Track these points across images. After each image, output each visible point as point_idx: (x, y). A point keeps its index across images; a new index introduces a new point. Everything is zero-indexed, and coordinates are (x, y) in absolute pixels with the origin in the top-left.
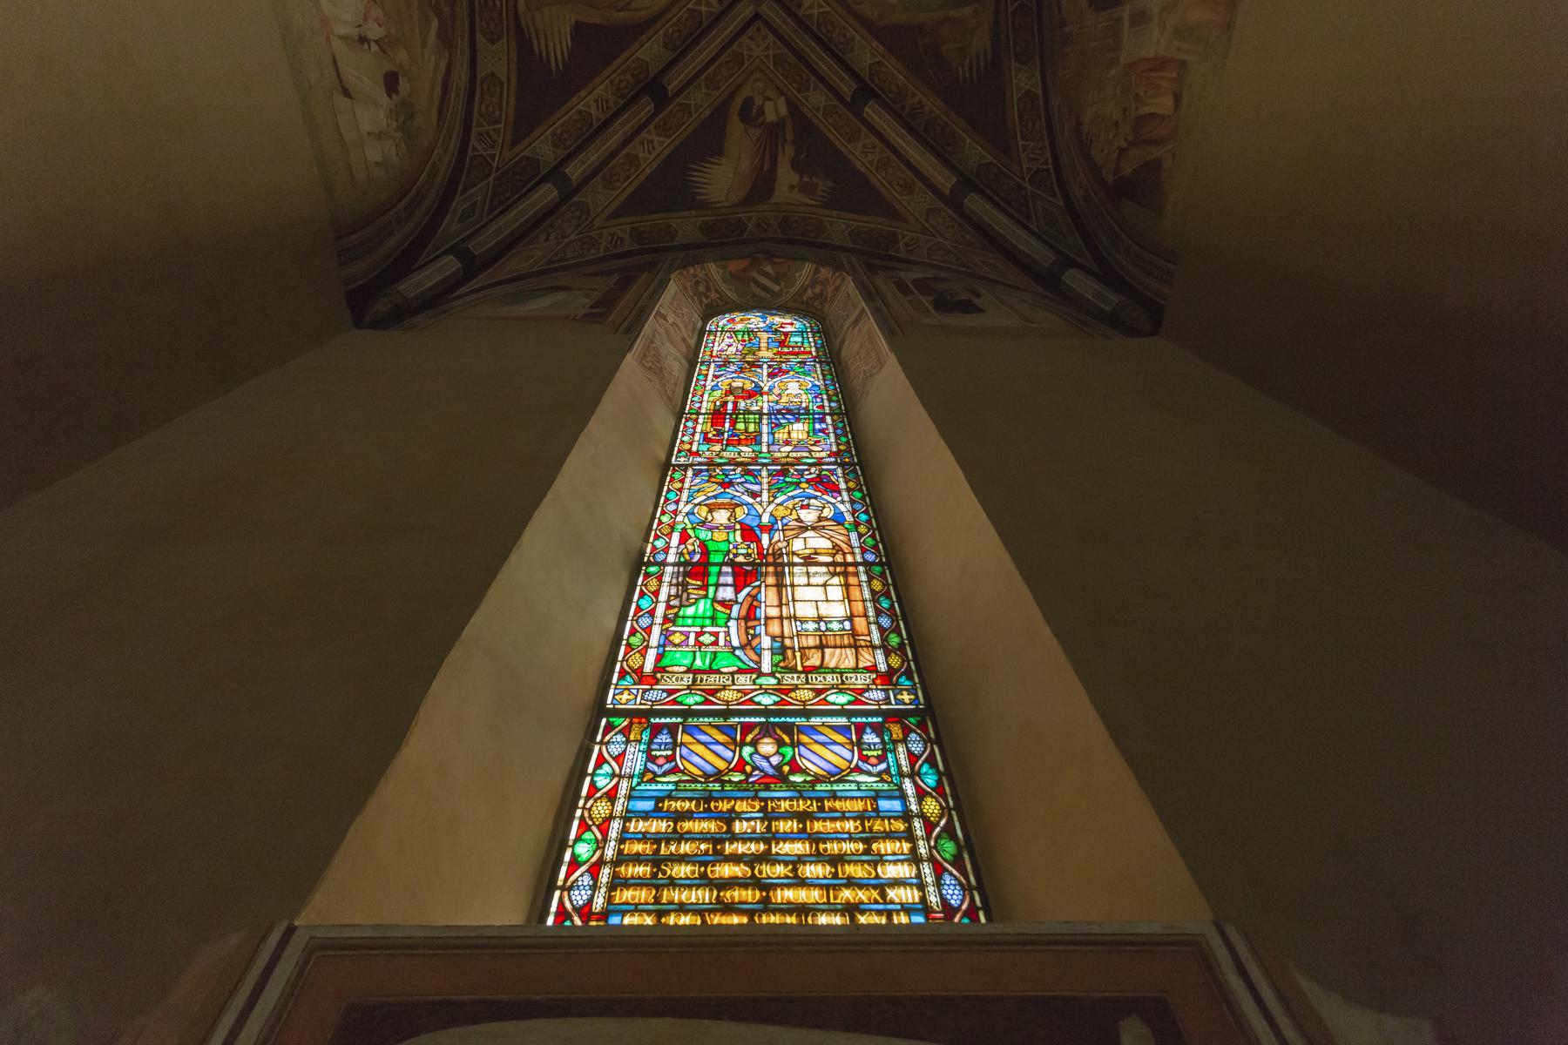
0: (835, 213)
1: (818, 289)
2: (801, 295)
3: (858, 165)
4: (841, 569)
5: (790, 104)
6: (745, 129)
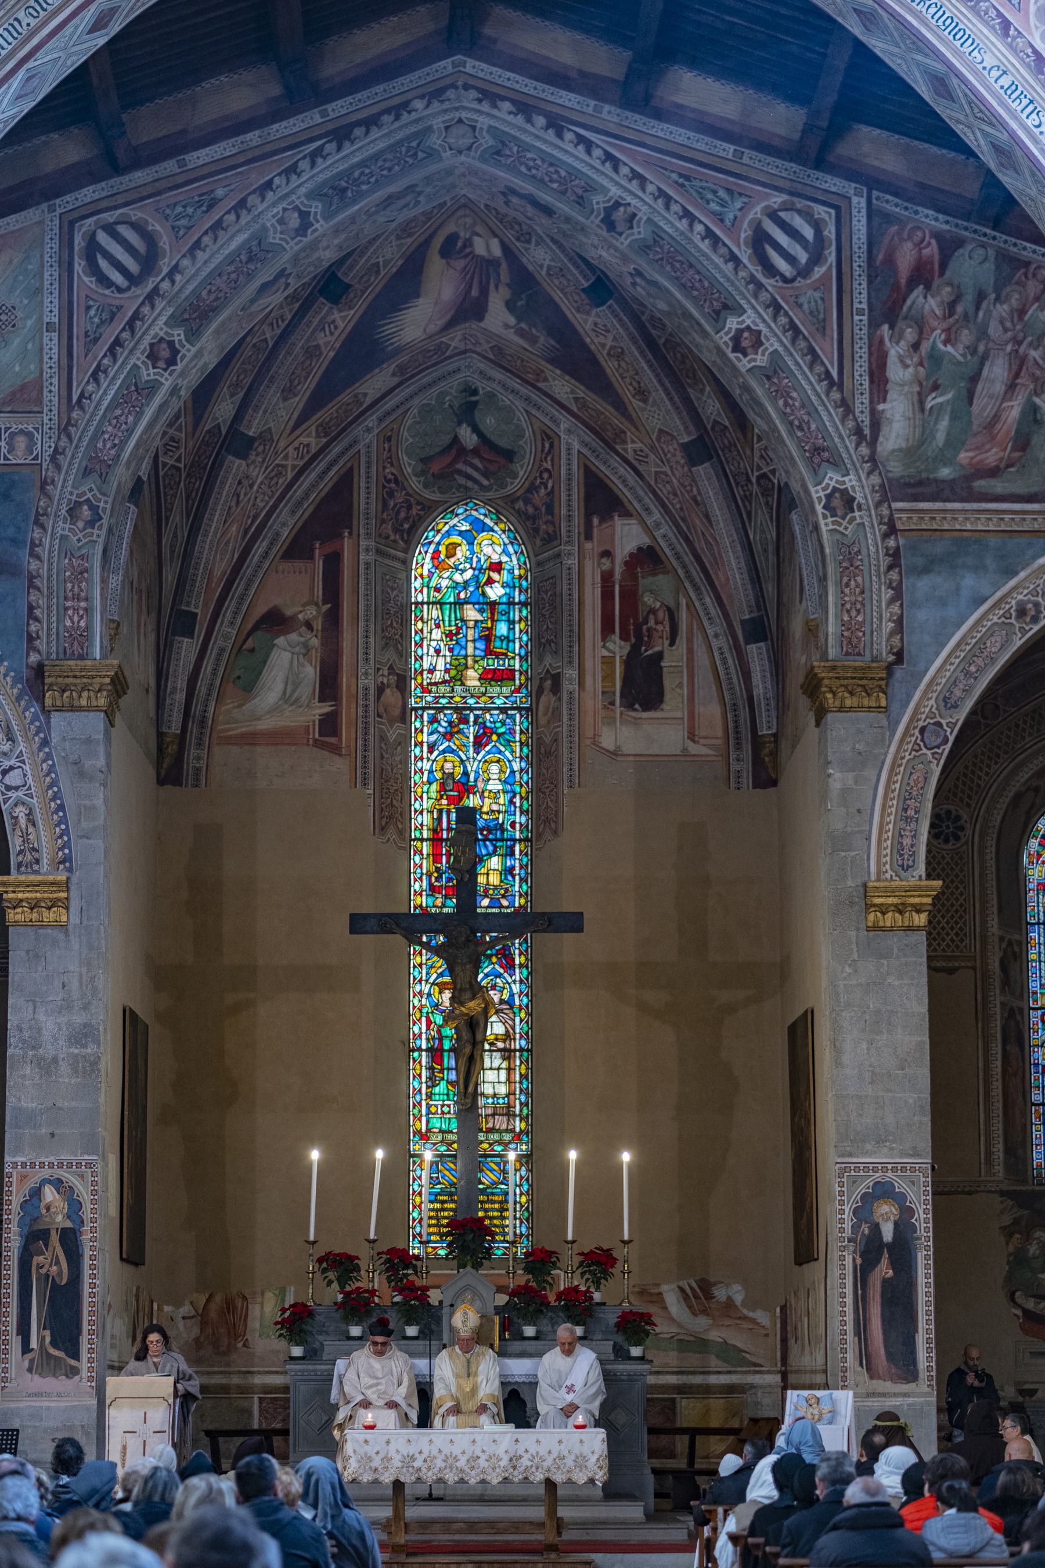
0: (558, 372)
2: (512, 502)
3: (588, 340)
4: (507, 1054)
5: (505, 248)
6: (448, 264)
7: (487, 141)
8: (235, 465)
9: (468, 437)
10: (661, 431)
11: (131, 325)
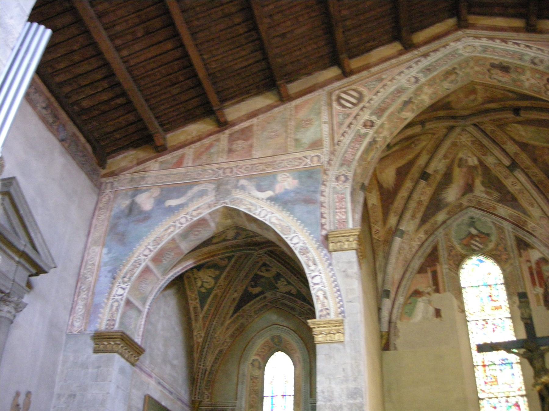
0: (500, 205)
1: (498, 253)
3: (510, 189)
5: (480, 161)
7: (480, 49)
8: (398, 240)
9: (474, 231)
10: (541, 217)
11: (355, 118)
